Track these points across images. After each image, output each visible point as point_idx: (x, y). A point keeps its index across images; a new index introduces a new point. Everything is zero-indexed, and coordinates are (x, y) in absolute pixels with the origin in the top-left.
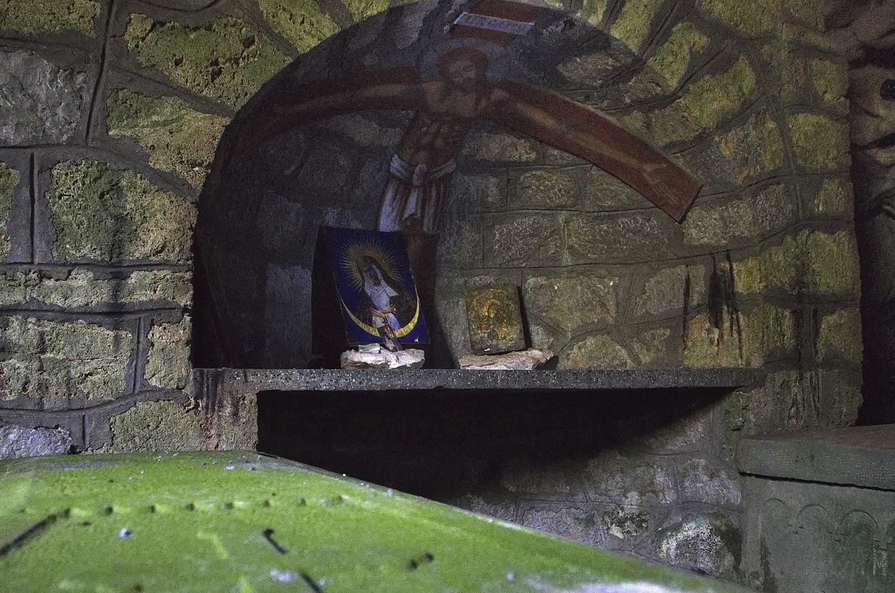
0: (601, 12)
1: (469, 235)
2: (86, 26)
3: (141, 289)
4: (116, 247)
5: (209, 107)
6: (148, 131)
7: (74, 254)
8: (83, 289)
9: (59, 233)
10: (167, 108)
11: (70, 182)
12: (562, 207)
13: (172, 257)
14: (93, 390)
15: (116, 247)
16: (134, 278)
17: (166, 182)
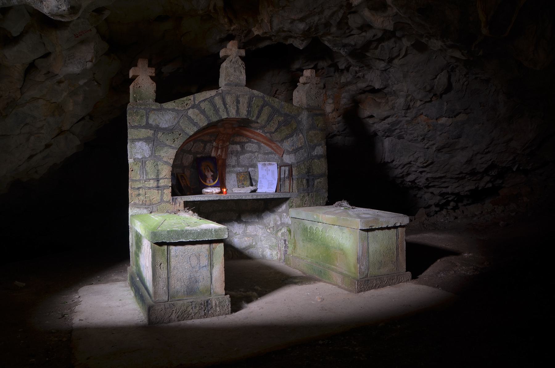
0: (255, 117)
1: (234, 158)
2: (151, 136)
3: (162, 183)
4: (158, 175)
5: (173, 148)
6: (162, 154)
7: (150, 177)
8: (152, 184)
9: (147, 174)
10: (165, 149)
11: (149, 165)
12: (256, 152)
13: (167, 177)
14: (154, 201)
15: (158, 175)
16: (161, 181)
17: (166, 163)
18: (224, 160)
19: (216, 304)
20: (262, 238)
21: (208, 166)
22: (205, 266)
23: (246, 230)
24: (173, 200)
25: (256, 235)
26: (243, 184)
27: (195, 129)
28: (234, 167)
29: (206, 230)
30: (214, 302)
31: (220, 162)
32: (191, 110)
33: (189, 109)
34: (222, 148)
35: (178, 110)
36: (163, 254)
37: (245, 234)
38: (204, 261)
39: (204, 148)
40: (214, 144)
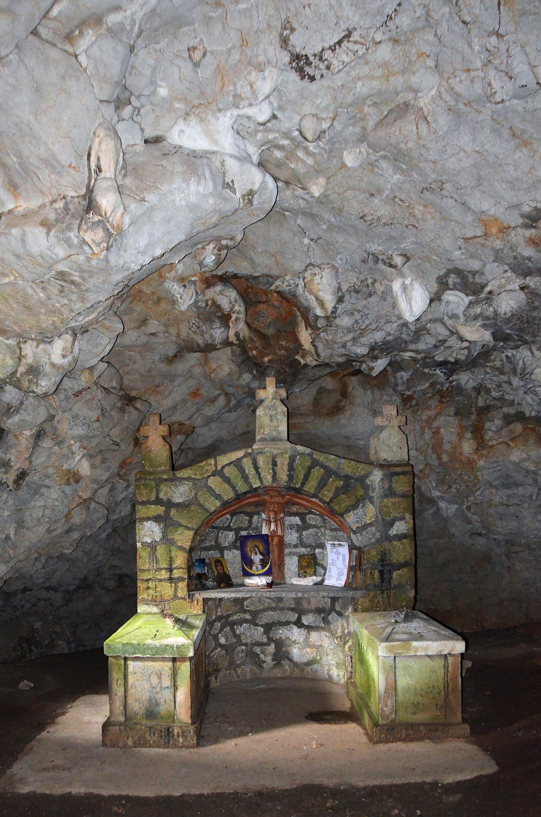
1: (295, 535)
18: (281, 538)
19: (178, 733)
20: (328, 650)
21: (256, 546)
22: (168, 687)
23: (309, 638)
24: (189, 596)
25: (321, 646)
26: (305, 572)
27: (218, 503)
28: (295, 546)
29: (166, 645)
30: (176, 731)
31: (276, 540)
32: (212, 477)
33: (209, 476)
34: (276, 521)
35: (195, 479)
36: (120, 669)
37: (307, 643)
38: (167, 682)
39: (250, 522)
40: (264, 516)
